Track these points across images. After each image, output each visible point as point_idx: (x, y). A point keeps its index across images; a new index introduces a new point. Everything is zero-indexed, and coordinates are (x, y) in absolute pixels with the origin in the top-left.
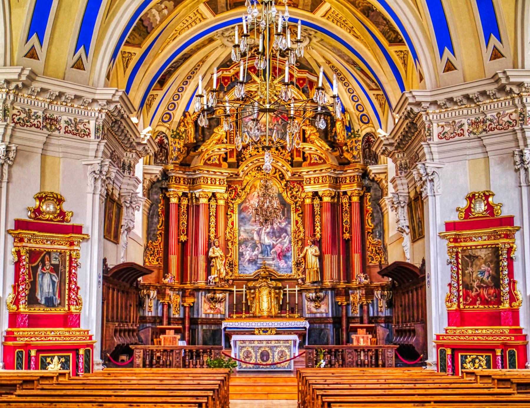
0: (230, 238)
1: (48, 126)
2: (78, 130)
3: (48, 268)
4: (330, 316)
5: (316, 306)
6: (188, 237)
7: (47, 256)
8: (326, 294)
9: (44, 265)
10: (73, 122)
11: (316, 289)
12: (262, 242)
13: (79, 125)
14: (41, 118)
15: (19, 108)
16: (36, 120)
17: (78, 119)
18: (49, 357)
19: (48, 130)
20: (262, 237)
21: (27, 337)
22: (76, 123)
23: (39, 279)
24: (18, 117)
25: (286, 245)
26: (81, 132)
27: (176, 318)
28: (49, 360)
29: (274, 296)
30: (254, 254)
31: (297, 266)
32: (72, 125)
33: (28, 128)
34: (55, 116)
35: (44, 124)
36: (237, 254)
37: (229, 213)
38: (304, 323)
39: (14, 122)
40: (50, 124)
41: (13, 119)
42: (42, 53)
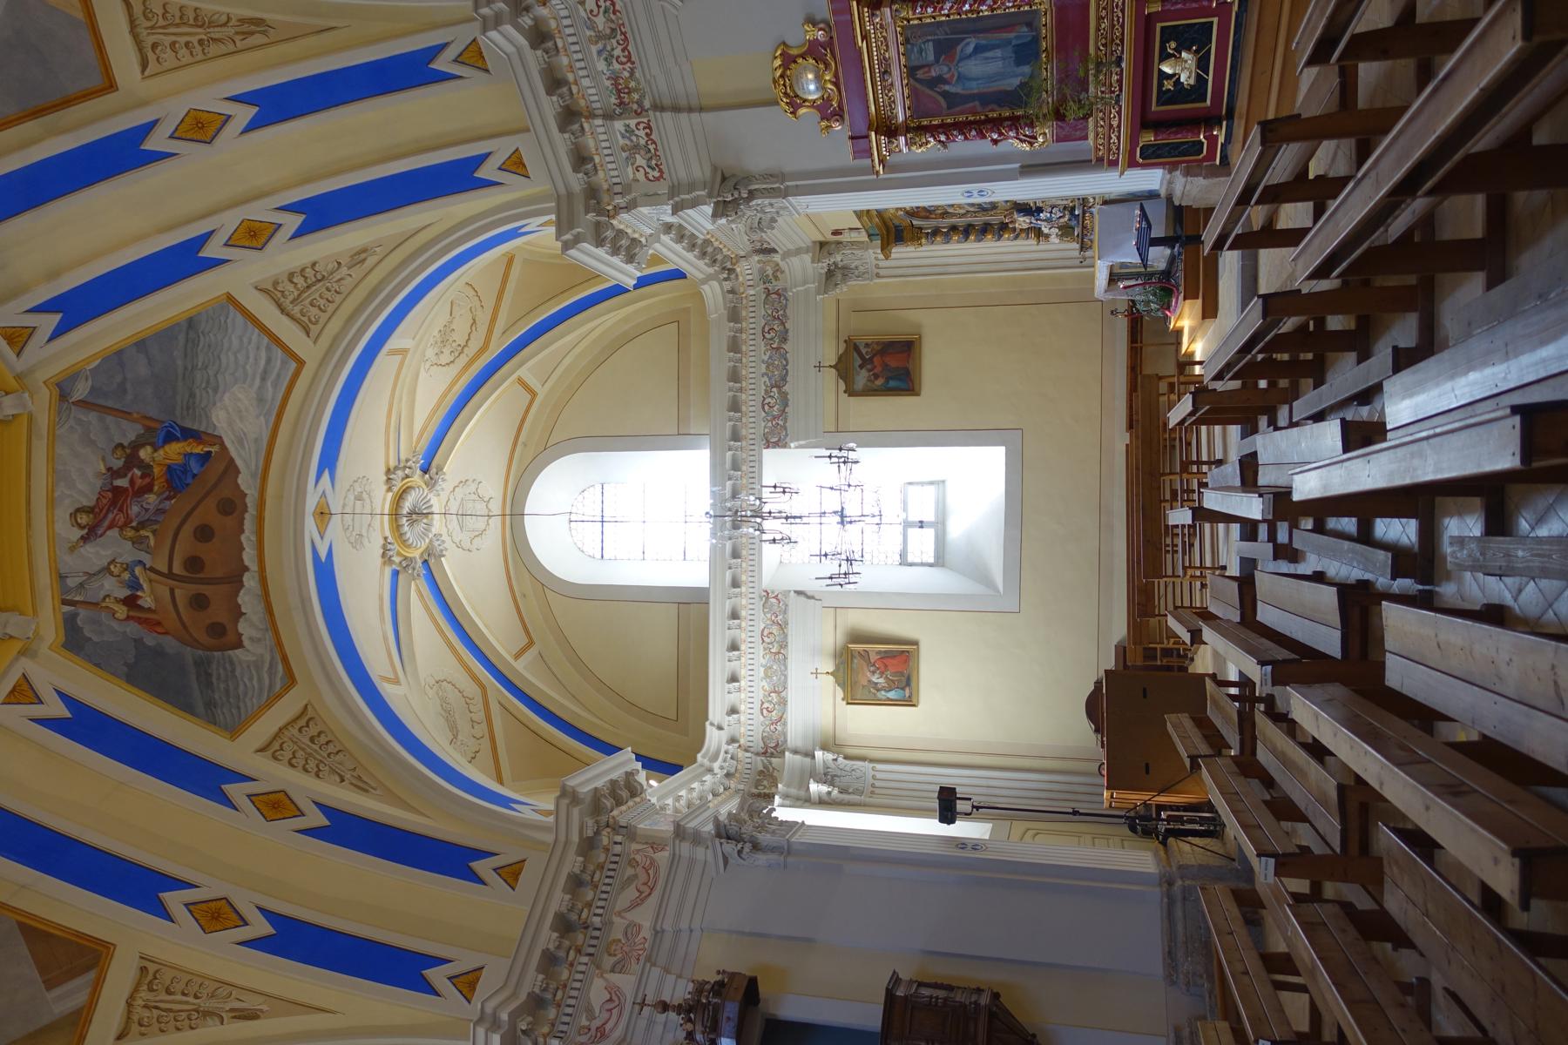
1: (636, 96)
2: (613, 30)
3: (945, 69)
7: (920, 74)
9: (941, 80)
10: (600, 46)
13: (601, 28)
14: (627, 122)
15: (630, 170)
16: (637, 132)
17: (589, 33)
18: (1160, 85)
19: (643, 96)
21: (1110, 138)
22: (600, 37)
23: (974, 87)
24: (648, 170)
26: (612, 21)
28: (1168, 85)
32: (609, 48)
33: (659, 147)
34: (608, 83)
35: (635, 106)
39: (661, 176)
40: (628, 93)
41: (657, 179)
42: (502, 149)
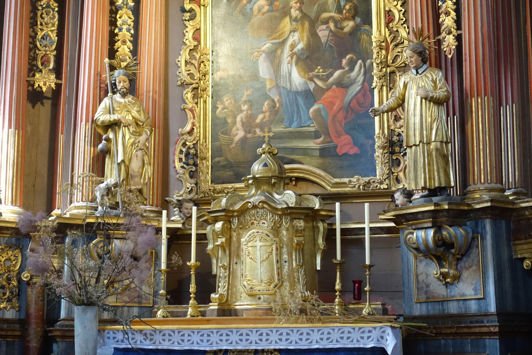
0: (188, 79)
4: (493, 309)
5: (444, 276)
6: (59, 76)
8: (475, 231)
11: (434, 214)
12: (282, 84)
20: (285, 67)
25: (356, 88)
27: (7, 321)
29: (291, 240)
30: (258, 121)
31: (392, 153)
36: (209, 123)
37: (187, 7)
38: (375, 334)
